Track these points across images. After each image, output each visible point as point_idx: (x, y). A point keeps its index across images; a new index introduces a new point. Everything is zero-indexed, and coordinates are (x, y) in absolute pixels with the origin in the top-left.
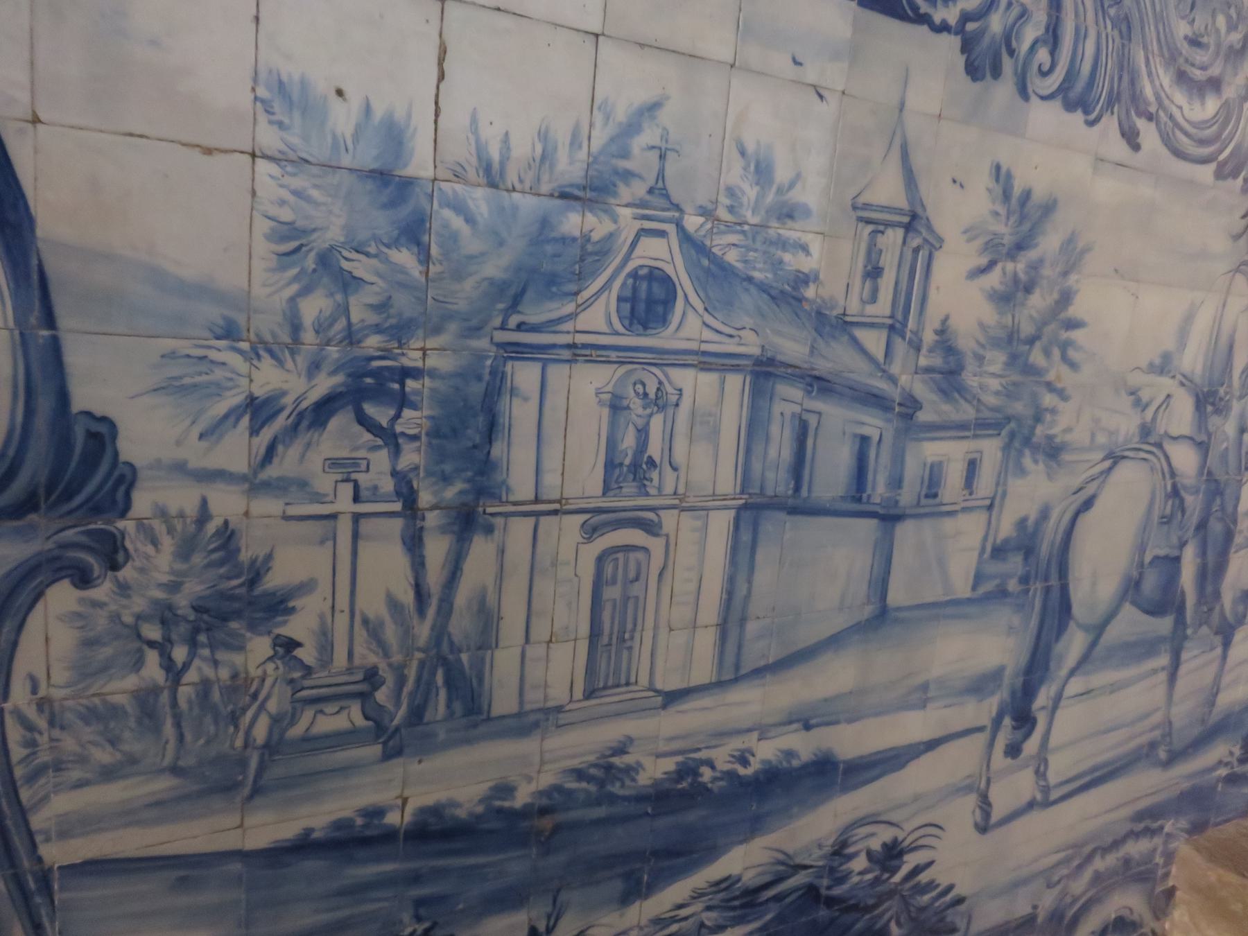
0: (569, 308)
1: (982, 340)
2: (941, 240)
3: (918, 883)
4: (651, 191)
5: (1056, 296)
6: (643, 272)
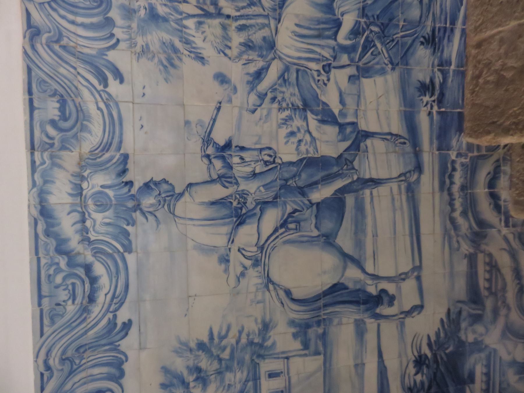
1: (221, 389)
3: (435, 342)
5: (200, 352)
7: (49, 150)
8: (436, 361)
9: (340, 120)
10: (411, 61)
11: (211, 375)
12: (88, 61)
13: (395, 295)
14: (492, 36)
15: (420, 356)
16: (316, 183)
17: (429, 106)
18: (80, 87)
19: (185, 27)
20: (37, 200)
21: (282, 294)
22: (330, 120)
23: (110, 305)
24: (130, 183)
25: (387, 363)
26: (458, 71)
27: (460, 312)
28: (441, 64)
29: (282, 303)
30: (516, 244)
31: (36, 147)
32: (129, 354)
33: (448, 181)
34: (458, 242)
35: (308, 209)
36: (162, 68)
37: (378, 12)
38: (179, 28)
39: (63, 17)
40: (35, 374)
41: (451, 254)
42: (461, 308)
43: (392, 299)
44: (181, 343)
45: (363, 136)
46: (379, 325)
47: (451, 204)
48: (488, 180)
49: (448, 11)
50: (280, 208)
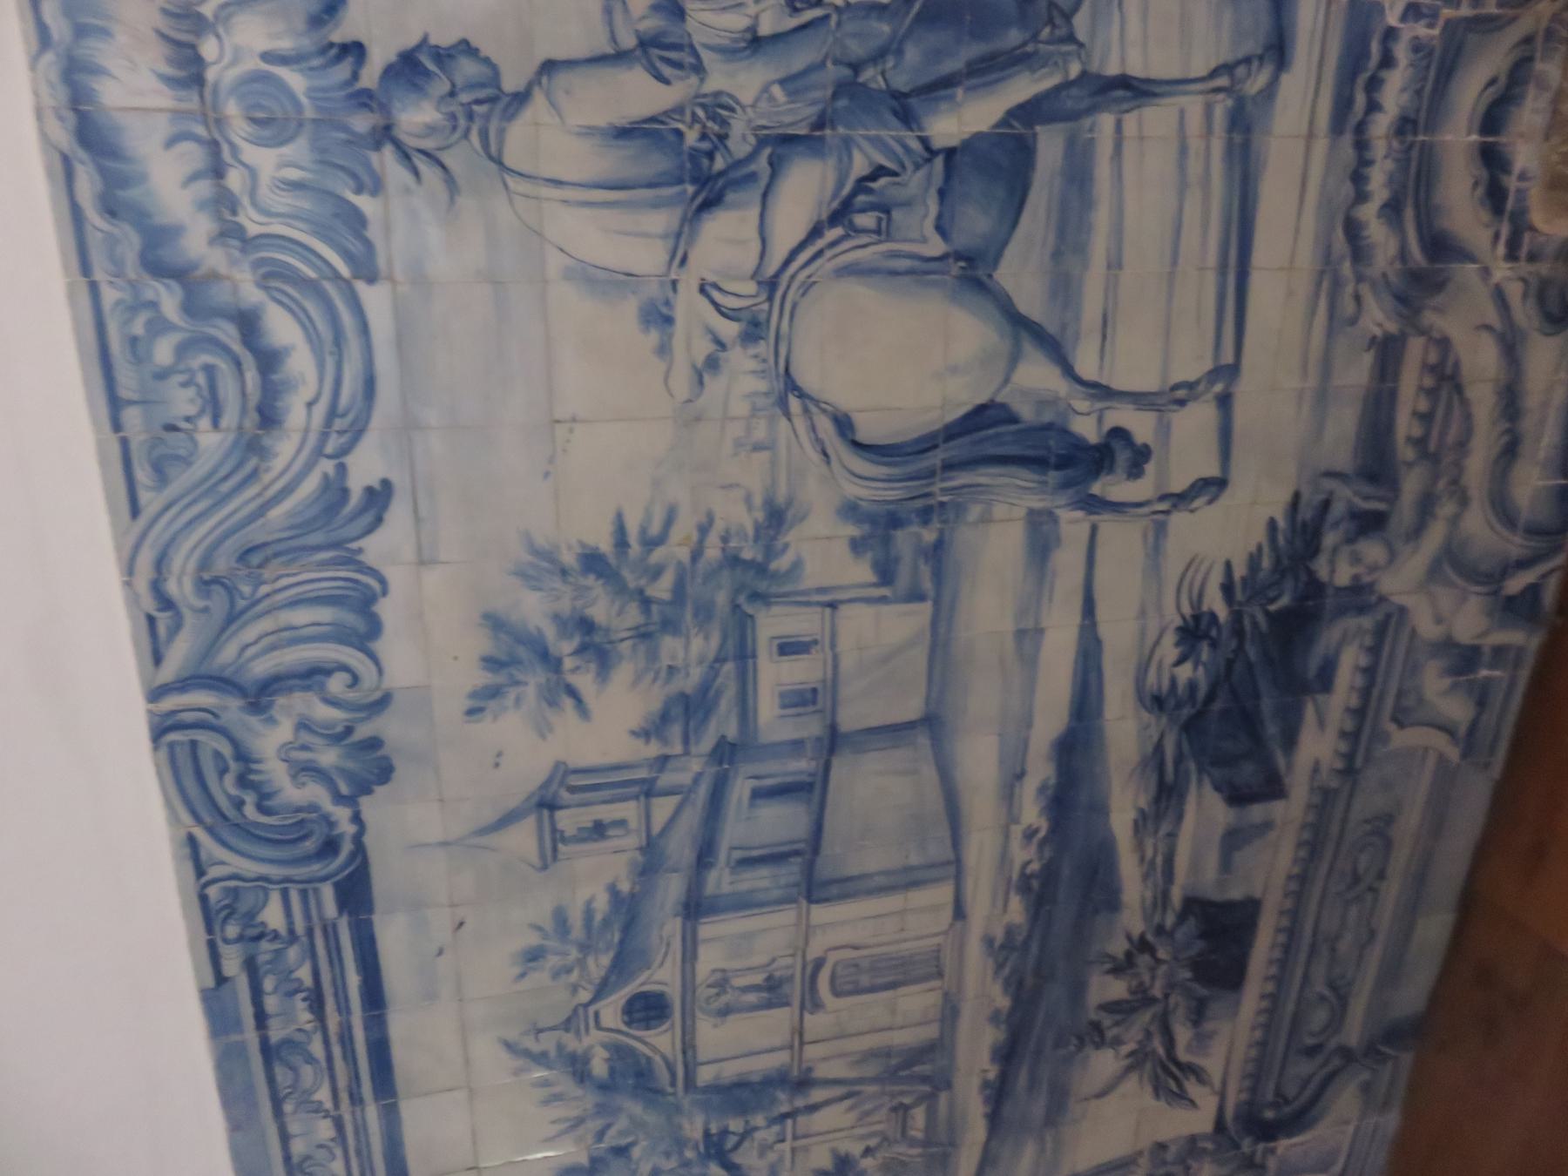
0: (657, 1058)
1: (651, 675)
2: (558, 764)
3: (1244, 579)
4: (567, 1030)
5: (590, 580)
6: (626, 1018)
8: (1238, 632)
11: (622, 640)
15: (1197, 618)
16: (948, 82)
20: (63, 94)
21: (826, 427)
23: (324, 436)
24: (355, 51)
25: (1105, 630)
27: (1326, 505)
29: (825, 454)
30: (1524, 313)
33: (1360, 99)
34: (1358, 298)
35: (917, 167)
41: (1330, 333)
42: (1331, 493)
43: (1140, 457)
44: (536, 552)
46: (1094, 530)
47: (1358, 178)
48: (1482, 108)
50: (832, 162)
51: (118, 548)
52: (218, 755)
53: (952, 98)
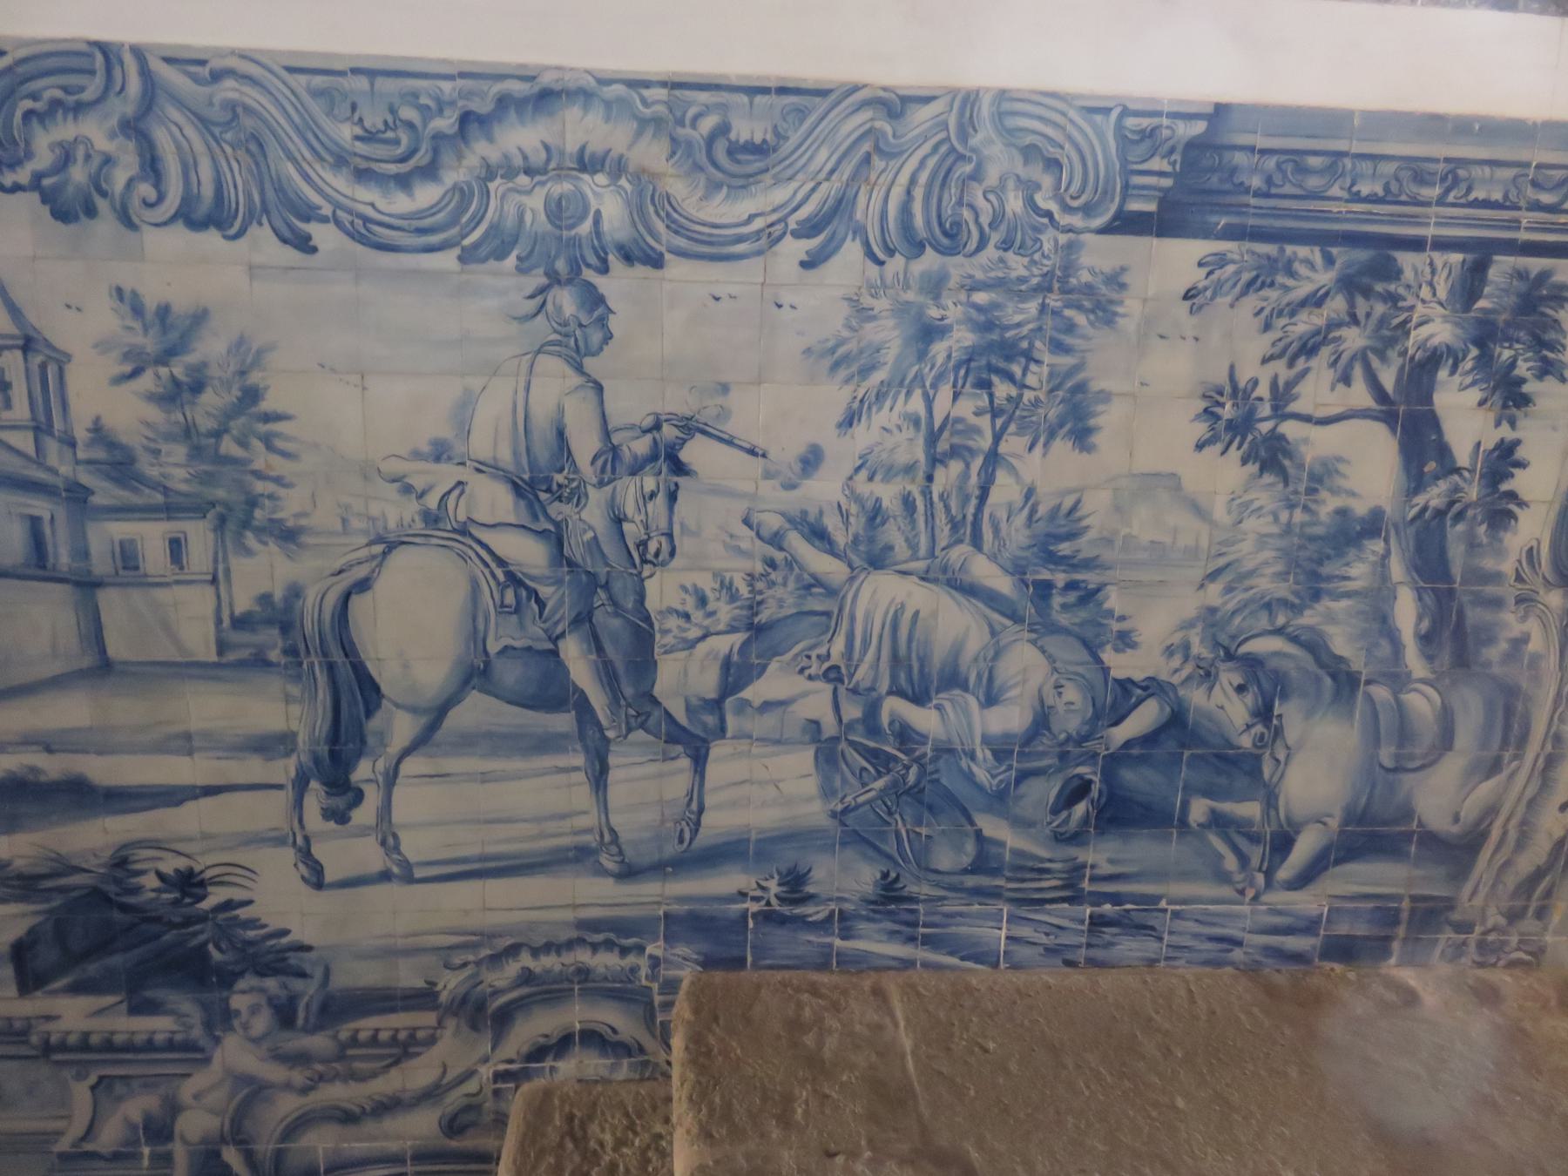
1: (151, 435)
2: (69, 357)
3: (236, 917)
5: (236, 392)
7: (671, 116)
8: (188, 921)
9: (729, 703)
10: (850, 853)
11: (184, 415)
12: (840, 207)
13: (351, 823)
14: (891, 1013)
15: (202, 884)
16: (600, 649)
17: (759, 893)
18: (794, 185)
19: (909, 394)
20: (572, 85)
21: (361, 572)
22: (730, 679)
23: (350, 212)
24: (604, 269)
25: (190, 806)
26: (829, 955)
27: (302, 975)
28: (843, 916)
29: (340, 572)
30: (454, 1099)
31: (677, 93)
32: (242, 243)
33: (599, 938)
34: (465, 965)
35: (546, 631)
36: (830, 344)
37: (944, 781)
38: (907, 382)
39: (922, 163)
40: (206, 49)
41: (437, 949)
42: (312, 977)
43: (339, 816)
44: (260, 353)
45: (697, 749)
46: (279, 787)
47: (548, 947)
49: (953, 929)
50: (547, 572)
51: (261, 51)
52: (82, 89)
53: (590, 652)
